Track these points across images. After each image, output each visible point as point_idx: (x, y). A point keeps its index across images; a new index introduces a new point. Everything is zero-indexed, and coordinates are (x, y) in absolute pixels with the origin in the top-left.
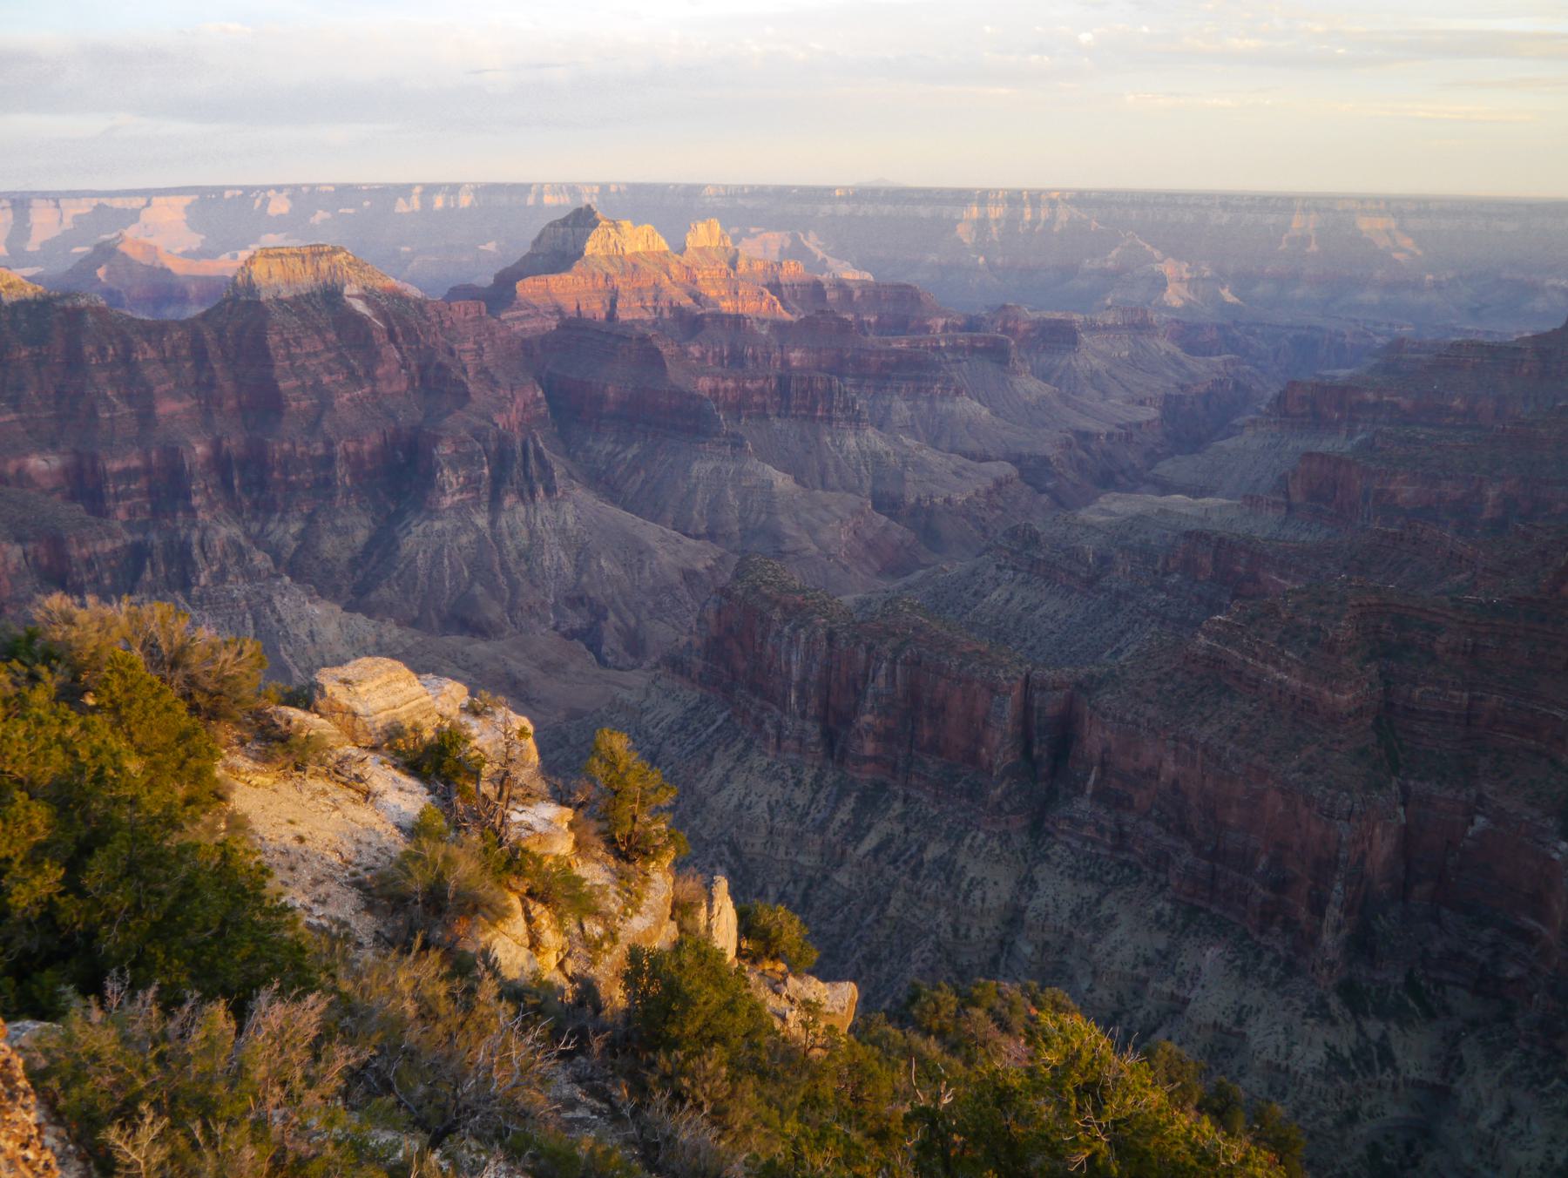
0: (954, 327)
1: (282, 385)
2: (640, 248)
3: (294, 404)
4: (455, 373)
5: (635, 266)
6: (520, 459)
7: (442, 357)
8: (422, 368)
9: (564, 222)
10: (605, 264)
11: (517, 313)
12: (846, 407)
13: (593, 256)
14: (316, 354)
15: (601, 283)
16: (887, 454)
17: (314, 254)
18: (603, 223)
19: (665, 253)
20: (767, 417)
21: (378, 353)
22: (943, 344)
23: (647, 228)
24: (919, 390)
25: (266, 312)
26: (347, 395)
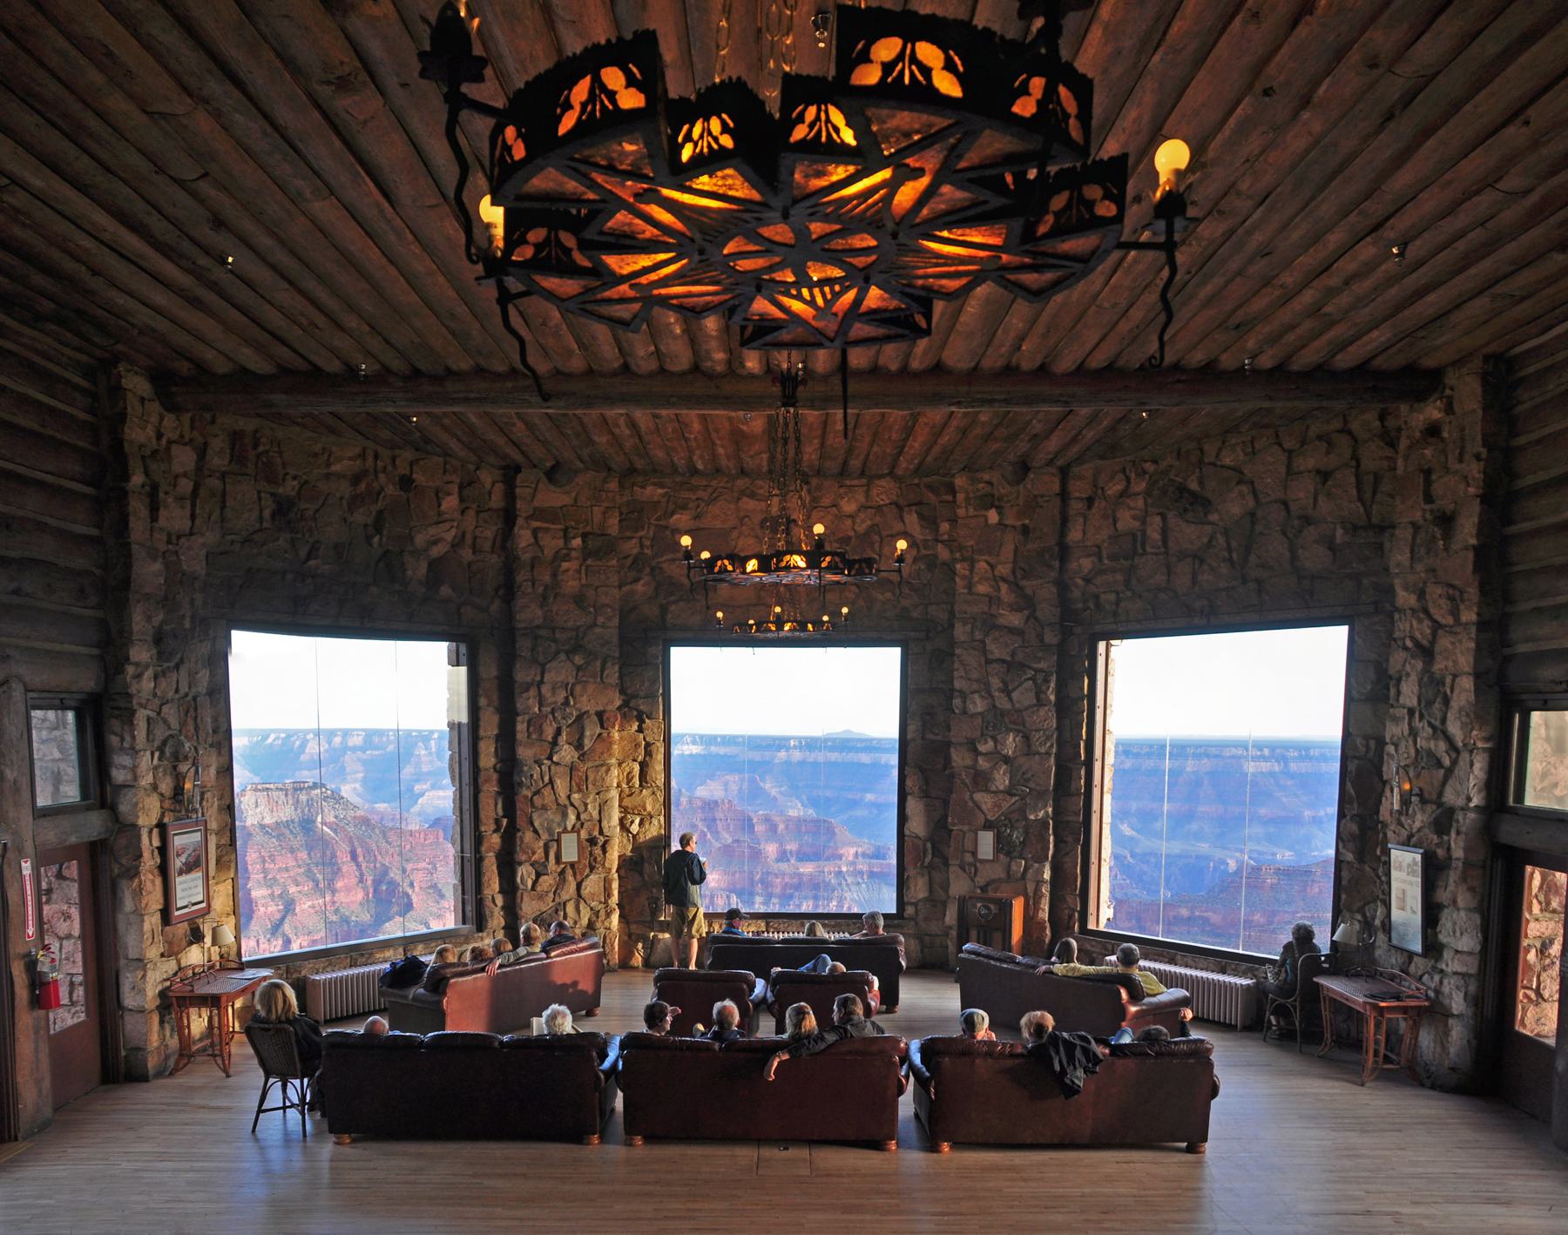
0: (864, 855)
7: (395, 874)
8: (377, 883)
17: (295, 789)
21: (339, 869)
22: (844, 869)
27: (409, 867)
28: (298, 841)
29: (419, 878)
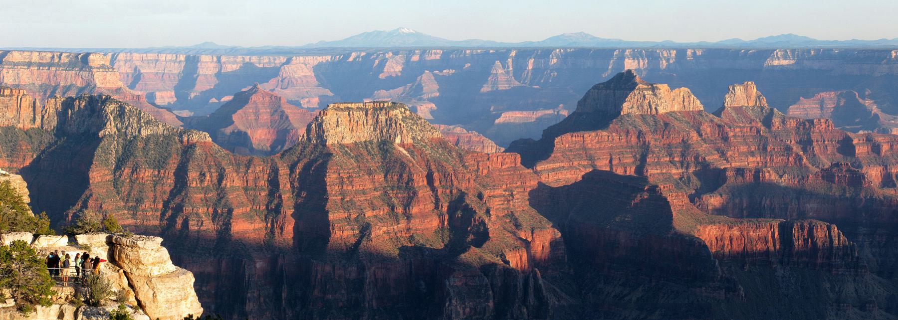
1: (331, 216)
2: (676, 108)
3: (339, 233)
4: (480, 213)
5: (666, 125)
6: (520, 294)
7: (471, 201)
8: (452, 210)
9: (607, 85)
10: (639, 122)
11: (552, 166)
13: (628, 115)
14: (364, 192)
15: (634, 139)
17: (375, 109)
18: (640, 86)
19: (700, 112)
21: (415, 193)
23: (684, 90)
25: (329, 155)
26: (385, 229)
27: (486, 193)
28: (375, 163)
29: (496, 205)
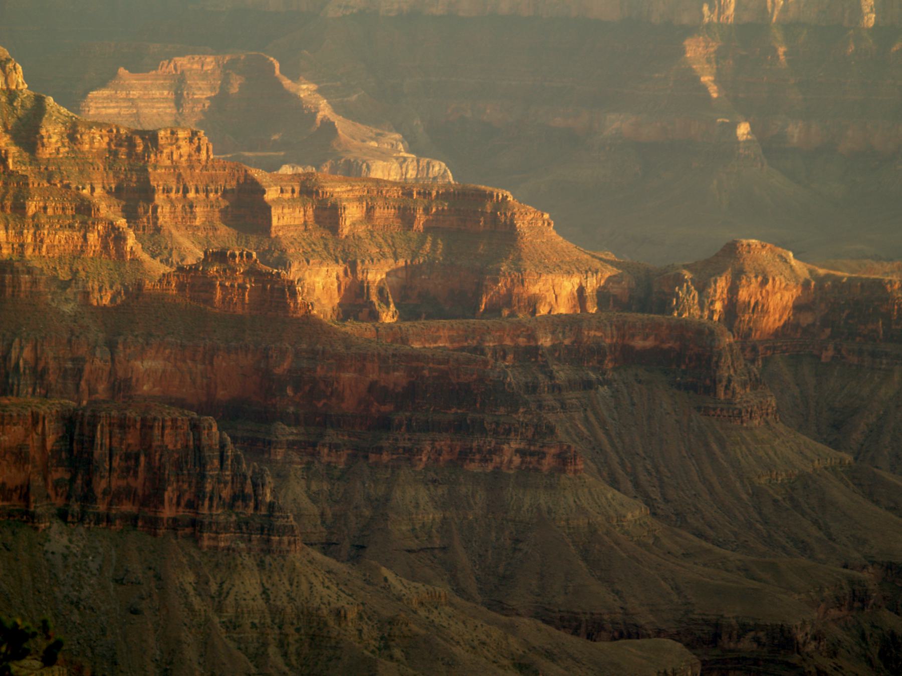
12: (239, 497)
16: (339, 615)
20: (30, 517)
22: (546, 341)
24: (465, 455)
